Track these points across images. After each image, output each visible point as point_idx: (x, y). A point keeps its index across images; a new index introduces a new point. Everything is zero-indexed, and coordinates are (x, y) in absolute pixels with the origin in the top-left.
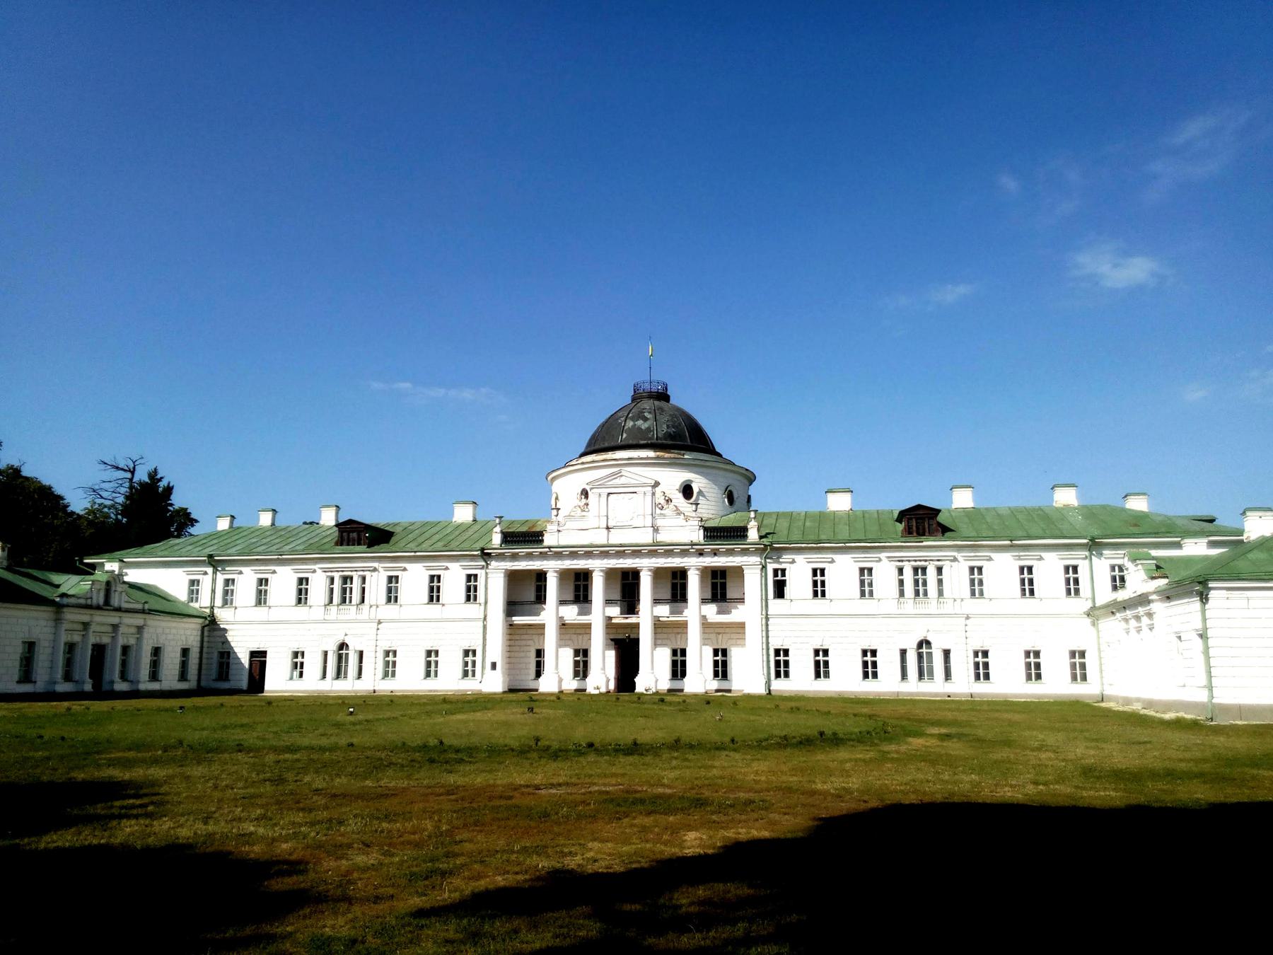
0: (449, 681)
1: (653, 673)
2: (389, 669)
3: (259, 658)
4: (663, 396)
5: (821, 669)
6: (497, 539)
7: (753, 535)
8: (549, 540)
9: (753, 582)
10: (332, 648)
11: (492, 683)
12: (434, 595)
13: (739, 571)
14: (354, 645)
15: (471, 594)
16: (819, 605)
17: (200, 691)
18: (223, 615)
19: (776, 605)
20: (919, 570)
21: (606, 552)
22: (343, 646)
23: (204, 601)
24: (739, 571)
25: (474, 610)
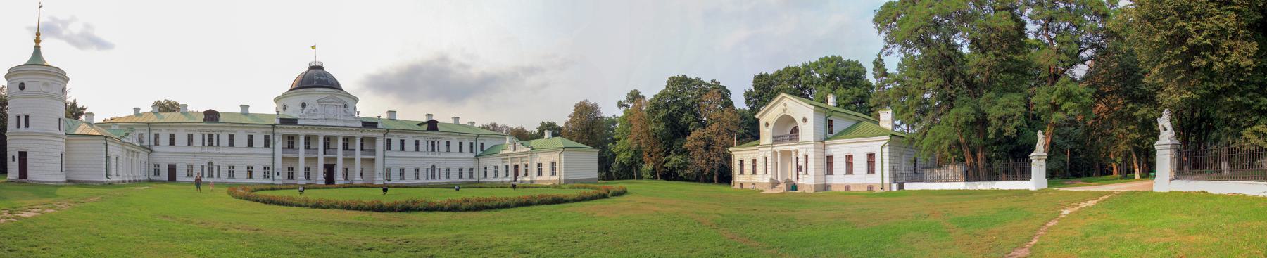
0: (258, 178)
1: (339, 178)
2: (231, 173)
3: (172, 169)
4: (321, 68)
5: (402, 175)
6: (278, 122)
7: (379, 126)
8: (300, 122)
9: (380, 145)
10: (206, 164)
11: (279, 180)
12: (250, 144)
13: (373, 140)
14: (215, 164)
15: (267, 145)
16: (402, 154)
17: (150, 181)
18: (155, 148)
19: (388, 153)
20: (433, 143)
21: (326, 127)
22: (210, 164)
23: (146, 143)
24: (373, 140)
25: (269, 151)
